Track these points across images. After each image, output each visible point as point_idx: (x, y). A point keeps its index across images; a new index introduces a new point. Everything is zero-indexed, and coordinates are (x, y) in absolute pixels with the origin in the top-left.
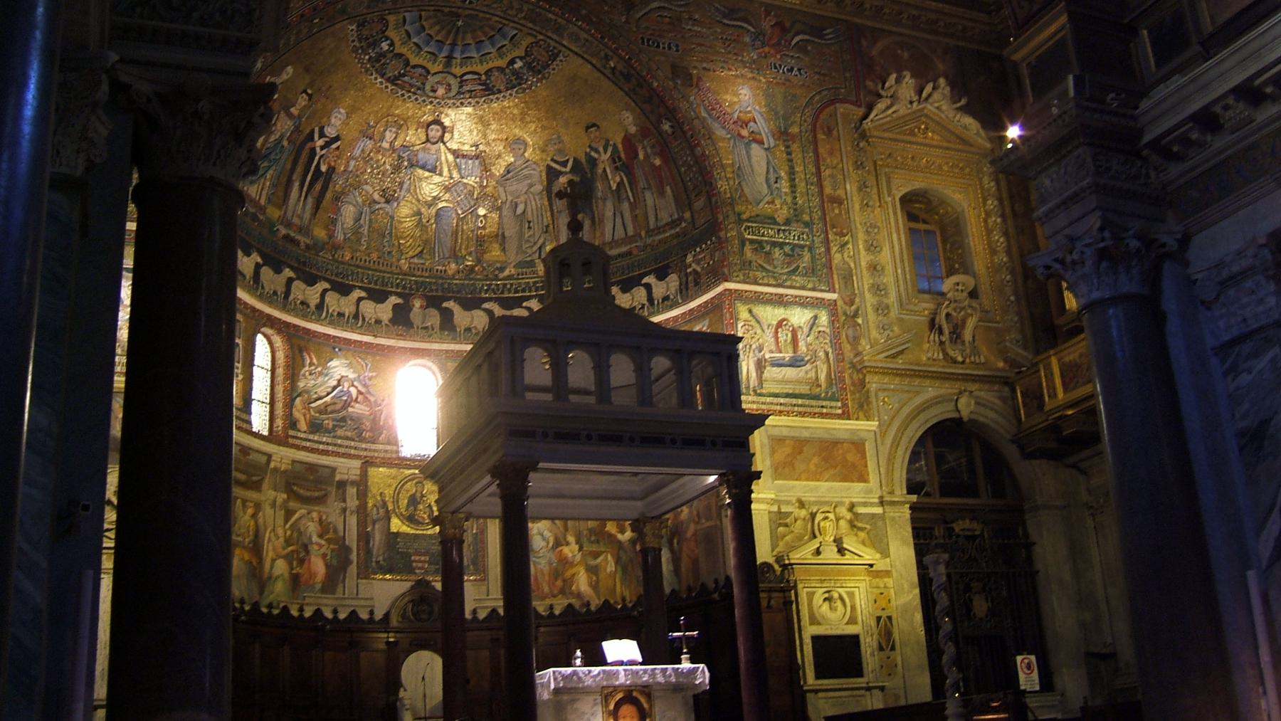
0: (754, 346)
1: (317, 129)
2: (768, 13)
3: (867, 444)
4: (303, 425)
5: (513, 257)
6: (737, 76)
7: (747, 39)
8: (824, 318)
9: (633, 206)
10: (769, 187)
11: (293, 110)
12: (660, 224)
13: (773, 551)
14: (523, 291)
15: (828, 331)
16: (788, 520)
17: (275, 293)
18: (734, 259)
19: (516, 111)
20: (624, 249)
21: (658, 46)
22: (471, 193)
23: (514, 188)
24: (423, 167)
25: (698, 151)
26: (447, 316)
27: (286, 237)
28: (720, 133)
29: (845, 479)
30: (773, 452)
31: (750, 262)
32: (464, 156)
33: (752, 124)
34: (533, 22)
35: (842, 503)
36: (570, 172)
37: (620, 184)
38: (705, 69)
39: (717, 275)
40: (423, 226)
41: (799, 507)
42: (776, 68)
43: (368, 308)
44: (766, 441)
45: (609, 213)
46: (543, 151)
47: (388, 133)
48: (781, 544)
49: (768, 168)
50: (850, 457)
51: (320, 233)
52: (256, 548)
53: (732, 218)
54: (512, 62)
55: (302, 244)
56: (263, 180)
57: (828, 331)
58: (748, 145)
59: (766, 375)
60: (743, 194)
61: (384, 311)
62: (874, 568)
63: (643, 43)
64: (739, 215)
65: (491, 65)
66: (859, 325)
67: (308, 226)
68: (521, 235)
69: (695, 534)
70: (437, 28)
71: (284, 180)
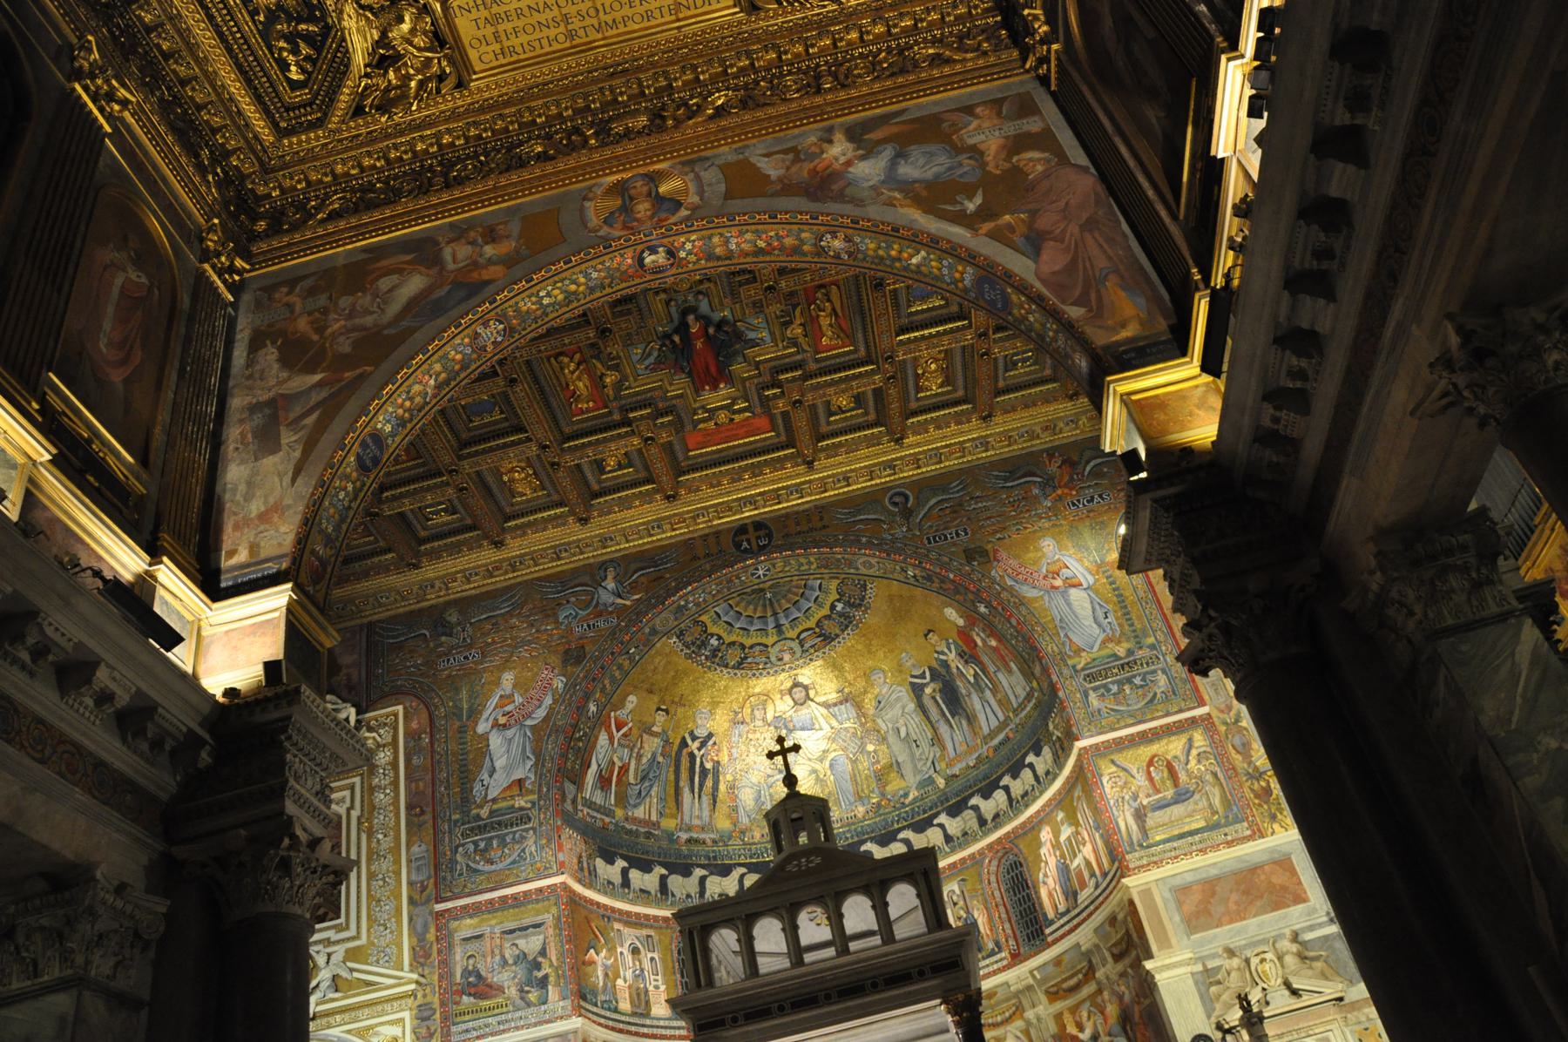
0: (1127, 797)
1: (687, 736)
2: (1051, 456)
3: (1293, 858)
5: (912, 780)
6: (1035, 532)
7: (1036, 491)
8: (1199, 739)
9: (994, 692)
10: (1099, 625)
11: (655, 729)
12: (1020, 700)
13: (1209, 1017)
14: (931, 809)
15: (1209, 749)
16: (1219, 976)
17: (688, 896)
18: (1077, 713)
19: (860, 647)
20: (1001, 737)
21: (946, 538)
22: (854, 734)
23: (889, 716)
24: (803, 729)
25: (1014, 622)
27: (689, 841)
28: (1029, 592)
29: (1277, 906)
30: (1180, 904)
31: (1099, 711)
32: (835, 705)
33: (1064, 570)
34: (826, 567)
35: (1281, 936)
36: (932, 680)
37: (976, 675)
38: (999, 539)
39: (1070, 737)
40: (822, 780)
41: (1229, 958)
42: (1074, 504)
44: (1168, 895)
45: (978, 706)
46: (901, 672)
47: (756, 712)
48: (1218, 1006)
49: (1093, 608)
50: (1276, 880)
51: (723, 824)
53: (1066, 672)
54: (833, 607)
55: (708, 841)
56: (648, 800)
57: (1209, 749)
58: (1065, 595)
59: (1150, 822)
62: (1347, 1001)
63: (930, 543)
64: (1074, 667)
65: (817, 617)
66: (1246, 729)
67: (710, 824)
68: (912, 755)
69: (1141, 1017)
70: (751, 607)
71: (672, 792)
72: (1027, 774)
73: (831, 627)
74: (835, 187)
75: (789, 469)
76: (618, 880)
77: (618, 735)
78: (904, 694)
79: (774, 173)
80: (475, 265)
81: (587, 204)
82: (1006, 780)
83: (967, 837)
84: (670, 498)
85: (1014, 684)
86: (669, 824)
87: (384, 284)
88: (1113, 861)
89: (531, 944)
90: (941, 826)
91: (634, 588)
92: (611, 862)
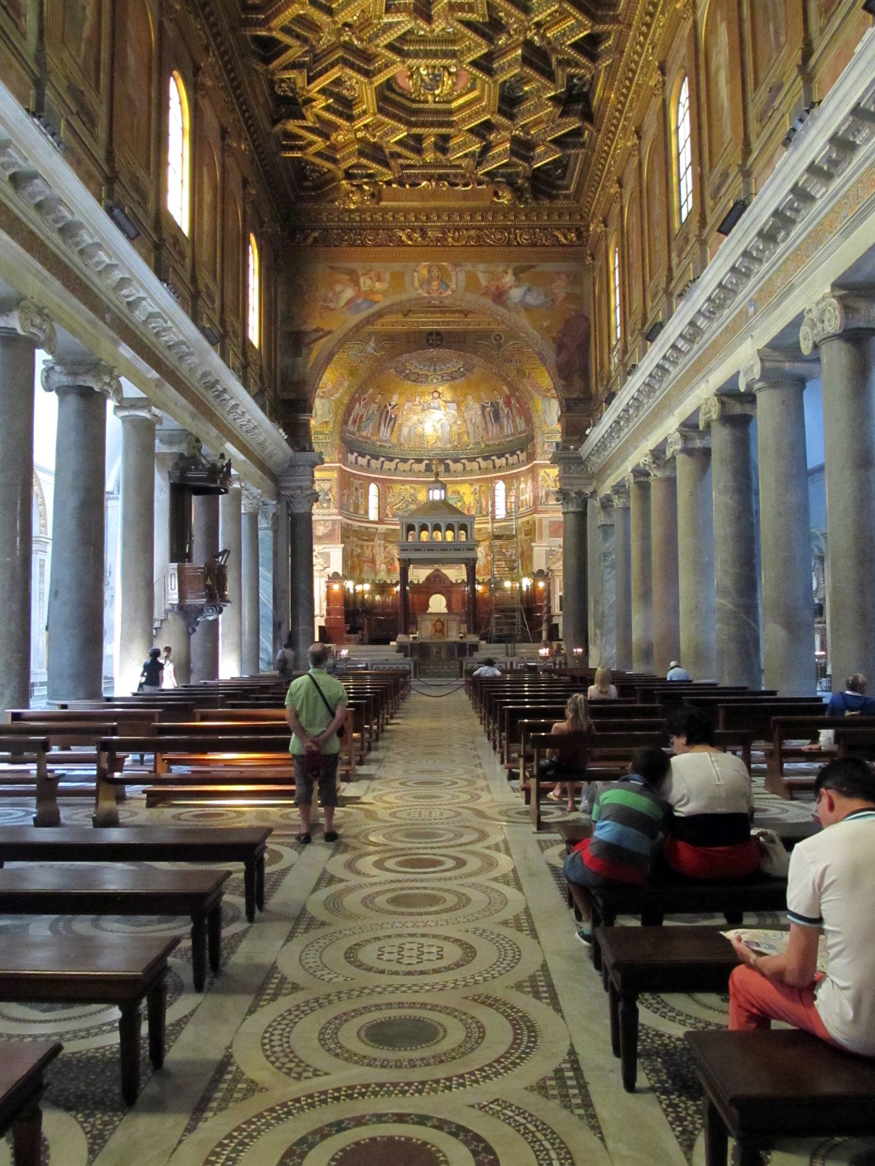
4: (390, 515)
5: (472, 441)
9: (514, 421)
13: (546, 564)
18: (539, 451)
24: (434, 408)
26: (447, 466)
27: (381, 446)
30: (550, 527)
43: (416, 467)
45: (505, 423)
51: (394, 440)
52: (373, 561)
60: (545, 422)
61: (422, 467)
68: (475, 431)
72: (515, 457)
73: (455, 375)
74: (504, 298)
75: (457, 315)
76: (354, 461)
77: (362, 403)
78: (477, 407)
79: (484, 283)
80: (372, 292)
81: (416, 274)
82: (507, 455)
83: (487, 471)
84: (405, 315)
85: (521, 425)
86: (374, 438)
87: (338, 288)
88: (534, 505)
89: (326, 486)
90: (479, 462)
91: (382, 348)
92: (352, 454)
